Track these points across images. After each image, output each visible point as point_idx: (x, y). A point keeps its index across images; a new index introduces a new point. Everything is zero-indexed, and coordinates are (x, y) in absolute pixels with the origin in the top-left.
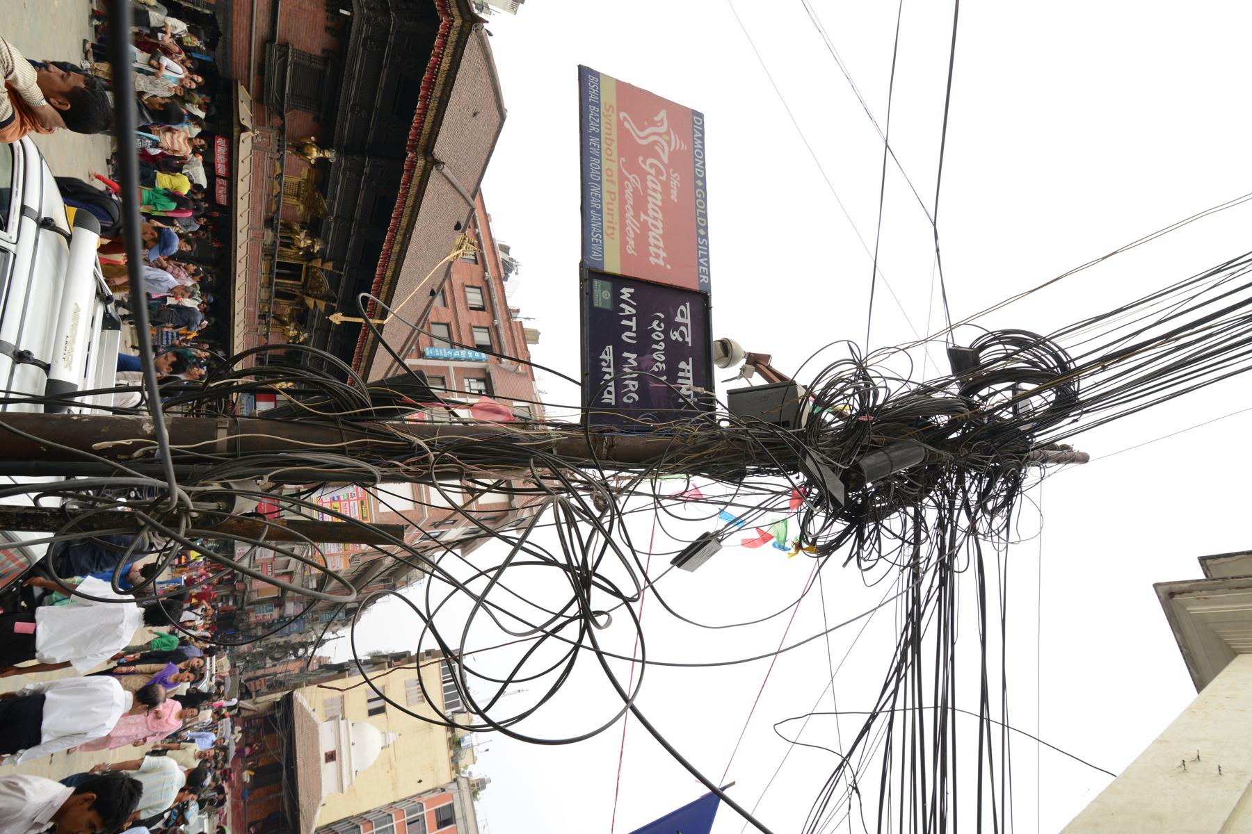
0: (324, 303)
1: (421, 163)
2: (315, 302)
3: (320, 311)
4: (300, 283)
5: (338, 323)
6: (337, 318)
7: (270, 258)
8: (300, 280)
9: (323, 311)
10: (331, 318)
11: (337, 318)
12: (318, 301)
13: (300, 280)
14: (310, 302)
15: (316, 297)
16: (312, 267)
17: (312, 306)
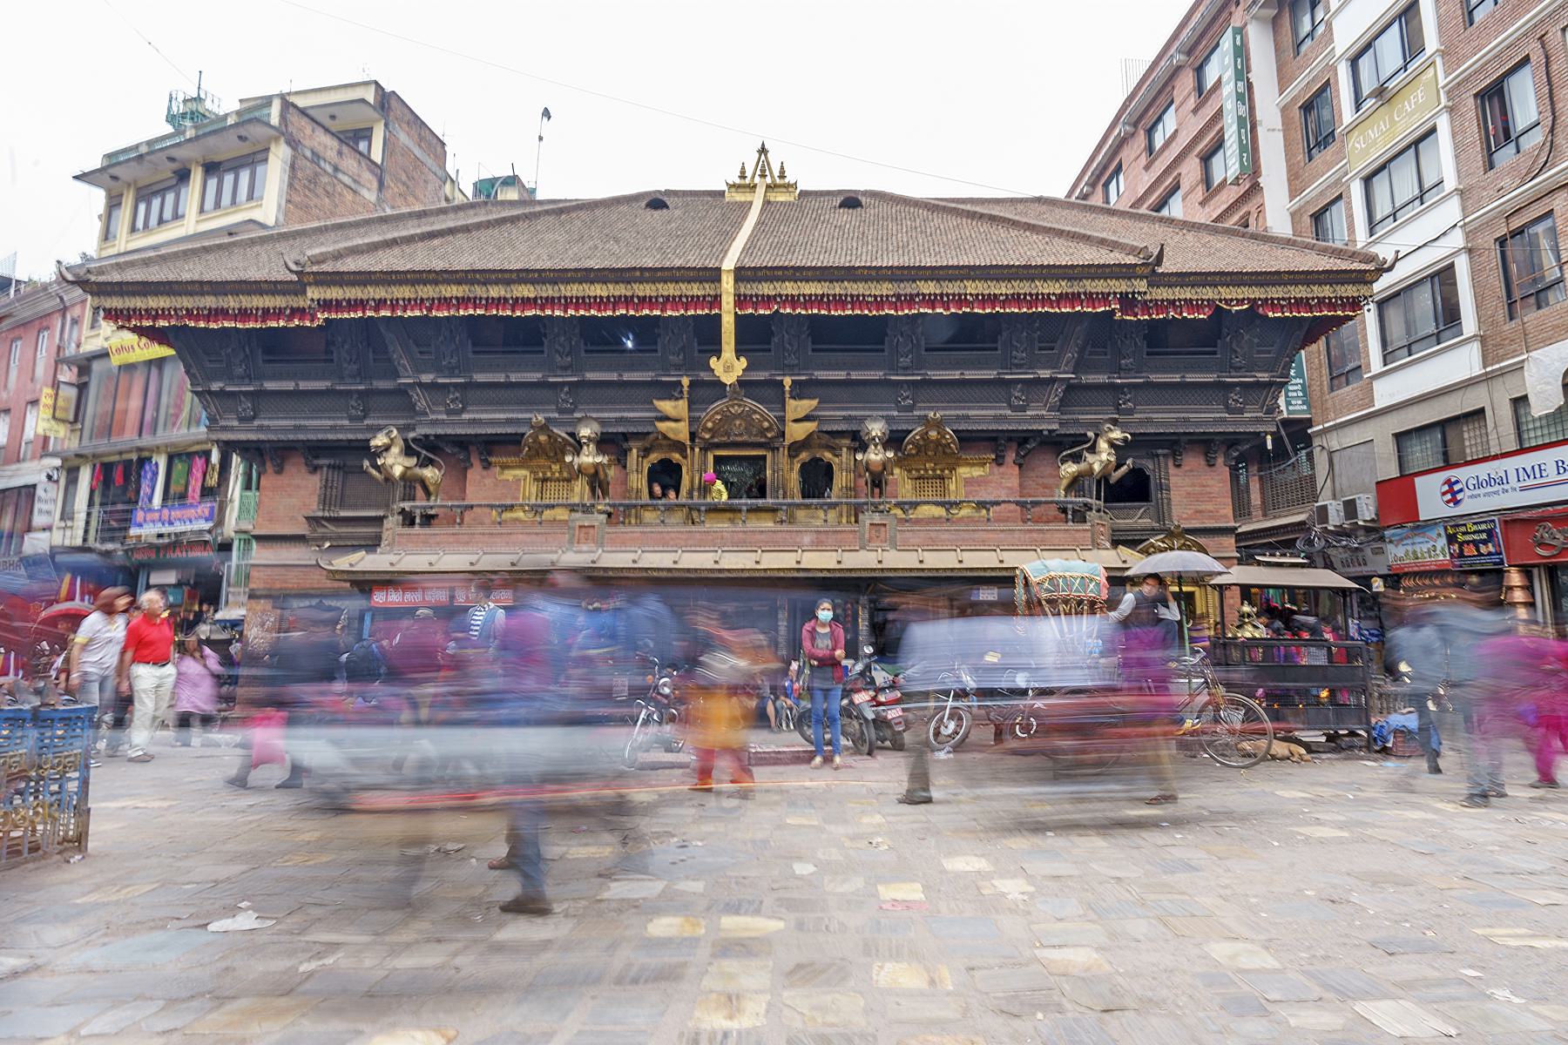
0: (792, 404)
1: (314, 293)
2: (796, 421)
3: (816, 409)
4: (769, 456)
5: (743, 362)
6: (729, 366)
7: (695, 514)
8: (764, 458)
9: (815, 402)
10: (729, 379)
11: (729, 366)
12: (790, 415)
13: (764, 458)
14: (797, 432)
15: (782, 420)
16: (693, 436)
17: (811, 426)
